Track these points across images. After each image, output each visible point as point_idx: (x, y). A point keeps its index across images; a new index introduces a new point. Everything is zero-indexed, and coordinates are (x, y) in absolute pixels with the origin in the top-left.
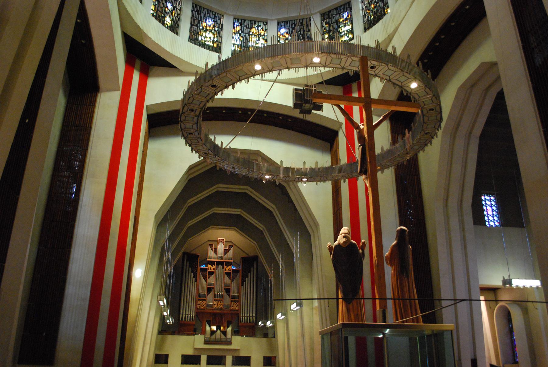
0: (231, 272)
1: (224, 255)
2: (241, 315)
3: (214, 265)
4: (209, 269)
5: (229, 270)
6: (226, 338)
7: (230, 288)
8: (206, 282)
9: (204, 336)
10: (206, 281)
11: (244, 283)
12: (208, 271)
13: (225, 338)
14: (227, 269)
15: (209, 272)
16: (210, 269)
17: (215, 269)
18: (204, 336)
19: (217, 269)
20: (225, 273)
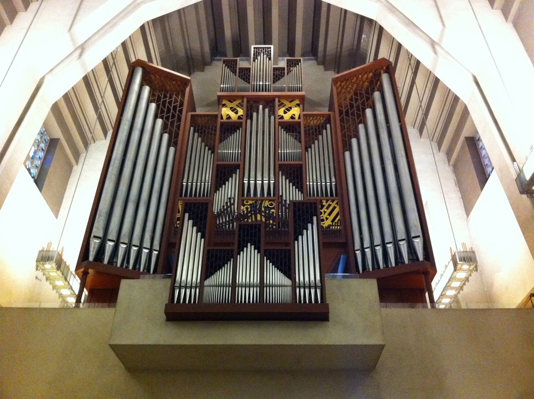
0: (301, 120)
1: (274, 82)
2: (357, 246)
3: (242, 109)
4: (224, 118)
5: (292, 118)
6: (294, 286)
7: (301, 165)
8: (213, 152)
9: (169, 282)
10: (212, 149)
11: (354, 141)
12: (219, 120)
13: (287, 281)
14: (285, 115)
15: (222, 124)
16: (229, 117)
17: (244, 118)
18: (169, 282)
19: (249, 116)
20: (280, 124)
